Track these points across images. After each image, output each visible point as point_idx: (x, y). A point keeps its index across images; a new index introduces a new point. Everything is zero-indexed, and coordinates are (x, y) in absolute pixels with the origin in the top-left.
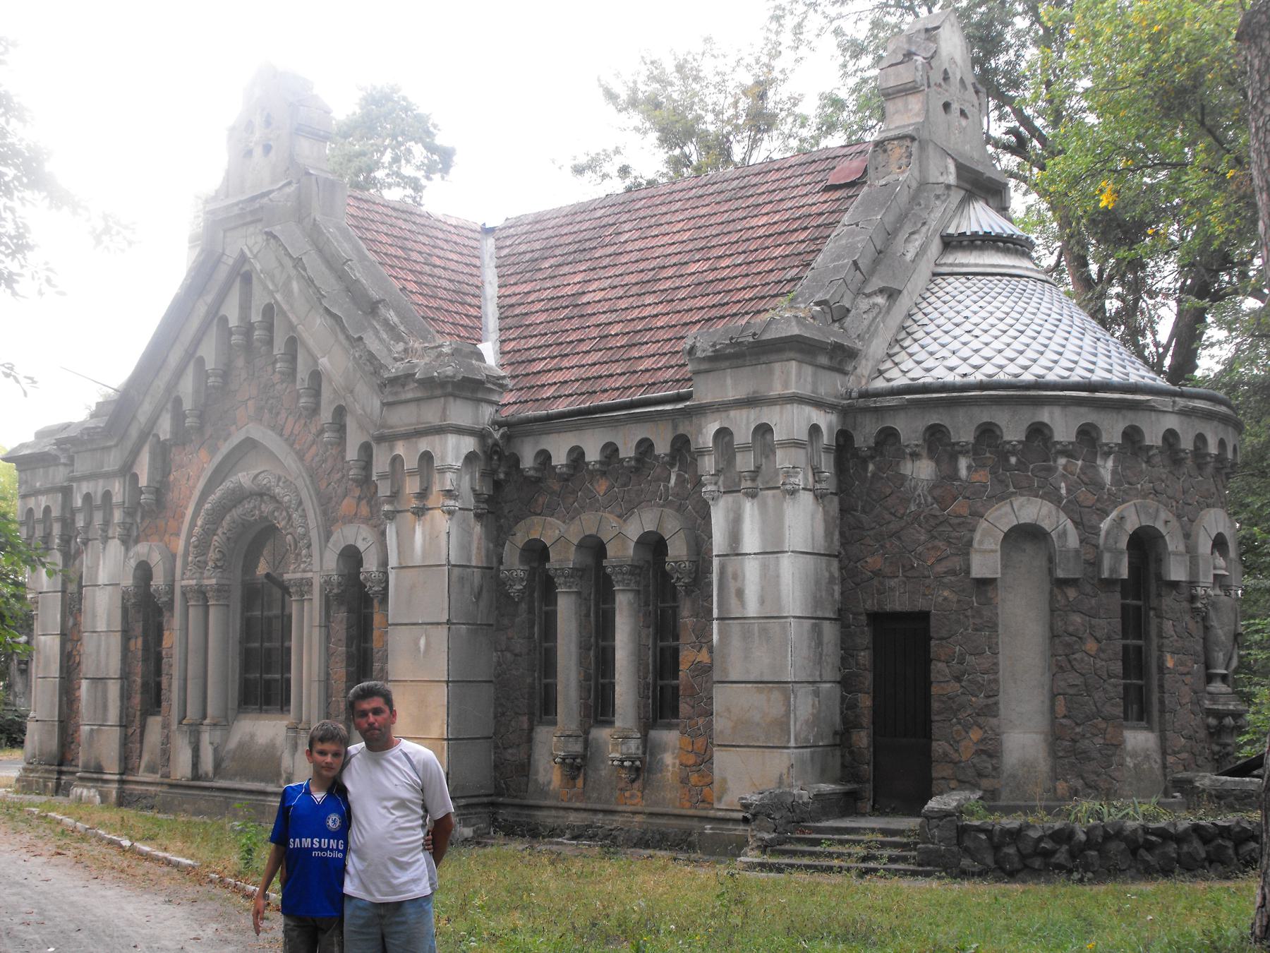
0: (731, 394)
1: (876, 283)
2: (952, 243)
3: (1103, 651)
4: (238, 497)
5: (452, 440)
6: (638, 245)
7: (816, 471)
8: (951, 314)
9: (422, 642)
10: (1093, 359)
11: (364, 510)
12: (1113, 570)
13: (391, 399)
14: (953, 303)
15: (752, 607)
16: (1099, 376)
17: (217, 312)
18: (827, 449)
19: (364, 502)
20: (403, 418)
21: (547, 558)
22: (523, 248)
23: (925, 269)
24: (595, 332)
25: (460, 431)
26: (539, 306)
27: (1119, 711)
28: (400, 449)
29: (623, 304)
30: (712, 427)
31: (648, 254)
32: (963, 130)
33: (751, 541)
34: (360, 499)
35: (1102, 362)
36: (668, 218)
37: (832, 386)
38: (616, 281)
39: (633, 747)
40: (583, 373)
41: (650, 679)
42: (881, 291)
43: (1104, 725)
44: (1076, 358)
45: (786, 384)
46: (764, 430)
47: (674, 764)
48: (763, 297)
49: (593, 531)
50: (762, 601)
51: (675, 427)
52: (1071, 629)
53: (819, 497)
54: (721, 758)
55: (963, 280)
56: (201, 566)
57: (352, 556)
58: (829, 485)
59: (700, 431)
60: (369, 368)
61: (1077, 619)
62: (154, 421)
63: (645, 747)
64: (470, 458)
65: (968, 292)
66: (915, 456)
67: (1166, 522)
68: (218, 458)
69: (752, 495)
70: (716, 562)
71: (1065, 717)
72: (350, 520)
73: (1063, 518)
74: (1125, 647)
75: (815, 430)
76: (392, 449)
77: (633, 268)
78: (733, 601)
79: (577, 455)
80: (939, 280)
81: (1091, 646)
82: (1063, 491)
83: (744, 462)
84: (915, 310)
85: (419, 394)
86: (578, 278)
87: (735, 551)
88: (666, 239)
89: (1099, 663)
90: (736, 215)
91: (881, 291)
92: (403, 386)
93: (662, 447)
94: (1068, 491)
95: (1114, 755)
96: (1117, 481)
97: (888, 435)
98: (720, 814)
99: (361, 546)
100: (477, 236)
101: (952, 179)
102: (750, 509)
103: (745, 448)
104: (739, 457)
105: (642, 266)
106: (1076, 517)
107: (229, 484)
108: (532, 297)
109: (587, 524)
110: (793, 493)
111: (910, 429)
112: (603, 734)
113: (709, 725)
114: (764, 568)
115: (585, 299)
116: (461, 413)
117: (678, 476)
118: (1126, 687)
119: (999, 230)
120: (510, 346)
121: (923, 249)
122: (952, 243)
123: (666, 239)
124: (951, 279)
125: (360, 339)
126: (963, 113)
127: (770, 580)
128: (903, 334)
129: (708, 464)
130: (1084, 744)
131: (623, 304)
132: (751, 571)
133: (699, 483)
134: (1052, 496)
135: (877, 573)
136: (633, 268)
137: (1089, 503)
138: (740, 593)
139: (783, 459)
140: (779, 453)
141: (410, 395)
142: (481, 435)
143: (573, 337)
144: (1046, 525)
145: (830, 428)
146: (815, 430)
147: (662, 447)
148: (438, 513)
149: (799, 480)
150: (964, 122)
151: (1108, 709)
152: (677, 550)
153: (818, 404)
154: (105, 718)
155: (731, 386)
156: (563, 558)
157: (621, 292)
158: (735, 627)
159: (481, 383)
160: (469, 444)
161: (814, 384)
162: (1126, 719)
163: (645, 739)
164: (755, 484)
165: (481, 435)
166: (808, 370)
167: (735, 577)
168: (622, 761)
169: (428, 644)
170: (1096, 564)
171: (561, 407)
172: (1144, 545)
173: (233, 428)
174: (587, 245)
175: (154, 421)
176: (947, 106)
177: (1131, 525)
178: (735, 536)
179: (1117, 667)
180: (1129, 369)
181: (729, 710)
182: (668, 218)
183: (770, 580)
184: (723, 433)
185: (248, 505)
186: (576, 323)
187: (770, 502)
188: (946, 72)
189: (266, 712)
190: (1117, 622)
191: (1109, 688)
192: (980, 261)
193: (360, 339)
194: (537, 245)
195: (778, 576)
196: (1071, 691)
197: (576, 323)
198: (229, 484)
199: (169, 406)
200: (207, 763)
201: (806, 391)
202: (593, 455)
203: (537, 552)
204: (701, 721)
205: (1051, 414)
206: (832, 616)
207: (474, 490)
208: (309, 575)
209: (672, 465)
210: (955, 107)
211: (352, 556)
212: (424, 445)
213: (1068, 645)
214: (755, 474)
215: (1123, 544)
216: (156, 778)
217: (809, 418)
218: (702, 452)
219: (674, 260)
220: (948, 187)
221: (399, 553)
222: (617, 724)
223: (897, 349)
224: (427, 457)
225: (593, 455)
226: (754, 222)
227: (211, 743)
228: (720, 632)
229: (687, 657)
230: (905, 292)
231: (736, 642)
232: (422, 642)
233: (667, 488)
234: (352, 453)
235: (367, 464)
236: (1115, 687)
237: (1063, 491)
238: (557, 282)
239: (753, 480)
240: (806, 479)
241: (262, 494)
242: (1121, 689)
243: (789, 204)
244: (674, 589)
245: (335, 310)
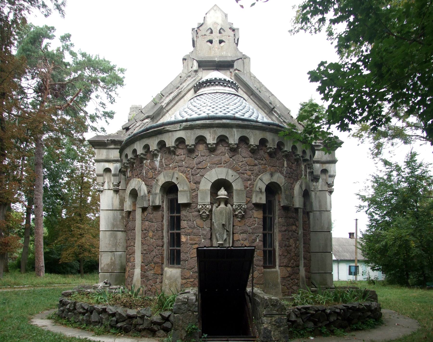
1: (146, 115)
3: (155, 236)
12: (153, 202)
18: (114, 175)
42: (148, 117)
61: (147, 223)
67: (177, 178)
71: (143, 262)
91: (148, 117)
95: (157, 278)
96: (161, 165)
137: (151, 177)
145: (116, 168)
150: (223, 44)
172: (170, 189)
201: (104, 157)
206: (123, 230)
215: (158, 190)
217: (104, 166)
220: (196, 71)
240: (109, 185)
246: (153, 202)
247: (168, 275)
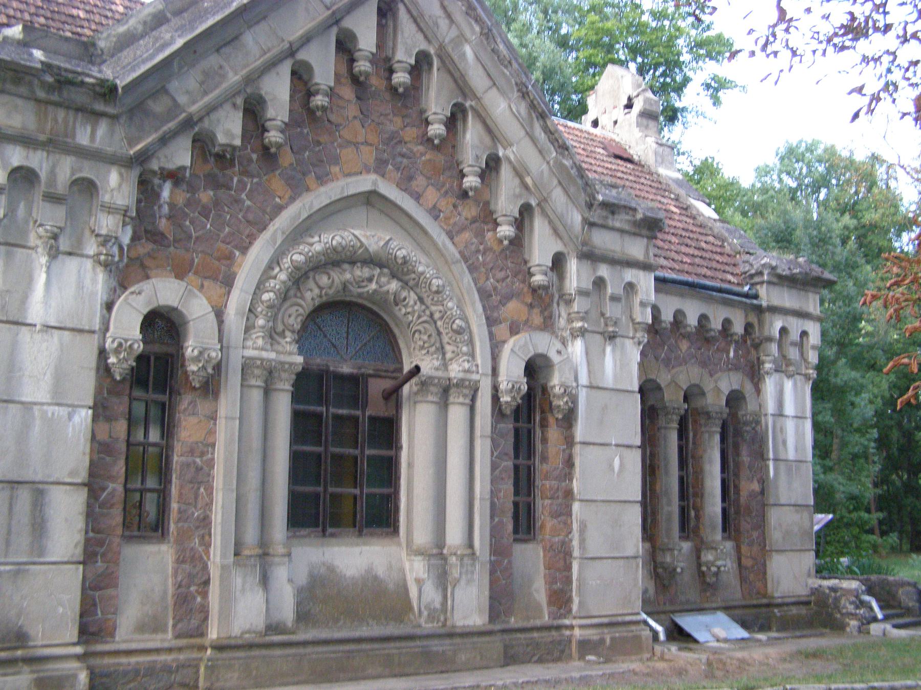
9: (617, 462)
11: (537, 319)
13: (595, 219)
17: (337, 22)
19: (536, 311)
20: (603, 240)
28: (604, 271)
30: (778, 324)
33: (789, 409)
34: (531, 306)
47: (732, 568)
49: (697, 382)
50: (796, 450)
51: (746, 316)
56: (273, 335)
69: (789, 376)
70: (770, 420)
76: (594, 270)
78: (781, 447)
79: (679, 316)
85: (627, 227)
87: (780, 414)
92: (613, 213)
98: (780, 600)
102: (788, 385)
113: (763, 537)
114: (797, 427)
117: (735, 351)
132: (790, 426)
138: (784, 442)
141: (618, 224)
147: (738, 328)
148: (628, 343)
156: (673, 398)
158: (782, 466)
164: (784, 367)
167: (781, 429)
169: (622, 465)
173: (335, 169)
178: (780, 404)
181: (780, 525)
183: (799, 435)
185: (361, 272)
187: (799, 384)
189: (332, 535)
195: (804, 434)
200: (287, 612)
202: (692, 320)
204: (755, 534)
208: (475, 377)
212: (630, 275)
218: (770, 339)
221: (589, 371)
224: (630, 287)
225: (692, 320)
227: (290, 581)
229: (747, 487)
231: (783, 477)
232: (617, 462)
244: (740, 433)
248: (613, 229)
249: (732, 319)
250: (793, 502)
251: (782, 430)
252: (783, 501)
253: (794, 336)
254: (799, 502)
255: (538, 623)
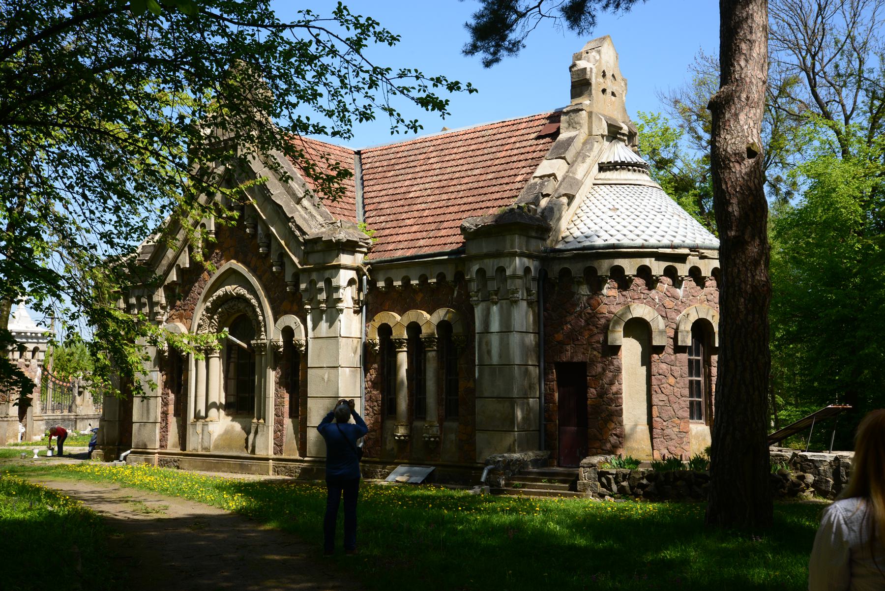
0: (485, 251)
2: (604, 167)
4: (227, 297)
5: (342, 271)
6: (439, 165)
7: (529, 291)
8: (601, 207)
9: (326, 377)
10: (676, 230)
11: (295, 308)
14: (603, 201)
15: (495, 360)
16: (677, 241)
18: (534, 279)
21: (391, 334)
22: (377, 164)
23: (589, 182)
24: (416, 214)
25: (346, 268)
26: (386, 198)
27: (687, 414)
29: (431, 199)
30: (476, 268)
31: (443, 171)
32: (612, 103)
33: (495, 326)
35: (681, 231)
36: (455, 150)
37: (537, 246)
38: (427, 186)
39: (435, 430)
40: (410, 237)
41: (444, 396)
43: (679, 421)
44: (666, 230)
45: (512, 247)
46: (502, 270)
48: (502, 198)
50: (500, 356)
52: (661, 372)
53: (530, 304)
54: (480, 437)
55: (608, 187)
57: (288, 333)
58: (534, 298)
59: (469, 270)
60: (297, 233)
62: (176, 258)
63: (441, 431)
64: (351, 282)
65: (611, 194)
66: (579, 283)
68: (214, 278)
72: (286, 313)
73: (656, 314)
74: (691, 382)
75: (527, 270)
77: (435, 178)
78: (486, 356)
80: (596, 187)
81: (672, 380)
82: (657, 301)
83: (492, 286)
84: (583, 204)
86: (407, 183)
87: (486, 331)
88: (454, 163)
89: (676, 389)
90: (490, 150)
93: (450, 277)
94: (660, 300)
97: (566, 272)
99: (293, 327)
100: (352, 156)
101: (606, 133)
102: (495, 309)
103: (493, 279)
104: (489, 284)
105: (440, 177)
106: (664, 314)
107: (220, 292)
108: (383, 193)
109: (412, 316)
110: (515, 302)
111: (576, 269)
112: (418, 424)
114: (501, 341)
115: (411, 195)
116: (345, 259)
118: (691, 403)
119: (629, 160)
120: (370, 220)
121: (587, 173)
122: (604, 167)
123: (454, 163)
124: (602, 187)
125: (293, 218)
126: (613, 94)
127: (505, 346)
128: (576, 217)
129: (473, 286)
130: (667, 431)
131: (431, 199)
132: (495, 340)
133: (469, 296)
134: (651, 303)
135: (559, 342)
136: (435, 178)
138: (489, 352)
139: (510, 285)
140: (509, 281)
141: (319, 248)
142: (358, 270)
143: (404, 216)
144: (648, 318)
145: (536, 269)
146: (527, 270)
147: (450, 277)
149: (519, 295)
150: (613, 98)
151: (681, 413)
152: (457, 329)
153: (529, 256)
154: (148, 418)
155: (486, 247)
157: (429, 192)
159: (357, 242)
160: (353, 274)
161: (527, 246)
162: (692, 417)
163: (441, 425)
165: (358, 270)
166: (524, 239)
168: (430, 438)
170: (675, 339)
171: (399, 254)
174: (412, 164)
175: (176, 258)
176: (604, 91)
177: (693, 318)
178: (486, 323)
179: (686, 392)
180: (697, 235)
182: (455, 150)
184: (481, 272)
186: (406, 209)
188: (604, 72)
190: (686, 369)
191: (681, 402)
192: (618, 177)
193: (293, 218)
194: (385, 163)
195: (508, 344)
196: (661, 403)
197: (406, 209)
198: (220, 292)
199: (186, 249)
203: (385, 330)
205: (650, 262)
207: (353, 298)
209: (455, 286)
210: (609, 91)
211: (288, 333)
212: (327, 274)
213: (660, 380)
214: (496, 293)
215: (689, 327)
216: (178, 450)
219: (457, 175)
220: (603, 136)
222: (428, 419)
223: (572, 225)
226: (499, 155)
228: (479, 372)
230: (577, 196)
232: (326, 377)
233: (452, 298)
234: (288, 278)
235: (297, 285)
236: (685, 402)
237: (657, 301)
238: (396, 185)
239: (496, 295)
240: (523, 294)
241: (240, 297)
242: (688, 403)
243: (518, 145)
245: (278, 202)
246: (683, 341)
247: (693, 433)
248: (318, 252)
249: (445, 272)
250: (495, 395)
251: (488, 344)
252: (486, 395)
253: (490, 272)
254: (502, 396)
255: (292, 457)
